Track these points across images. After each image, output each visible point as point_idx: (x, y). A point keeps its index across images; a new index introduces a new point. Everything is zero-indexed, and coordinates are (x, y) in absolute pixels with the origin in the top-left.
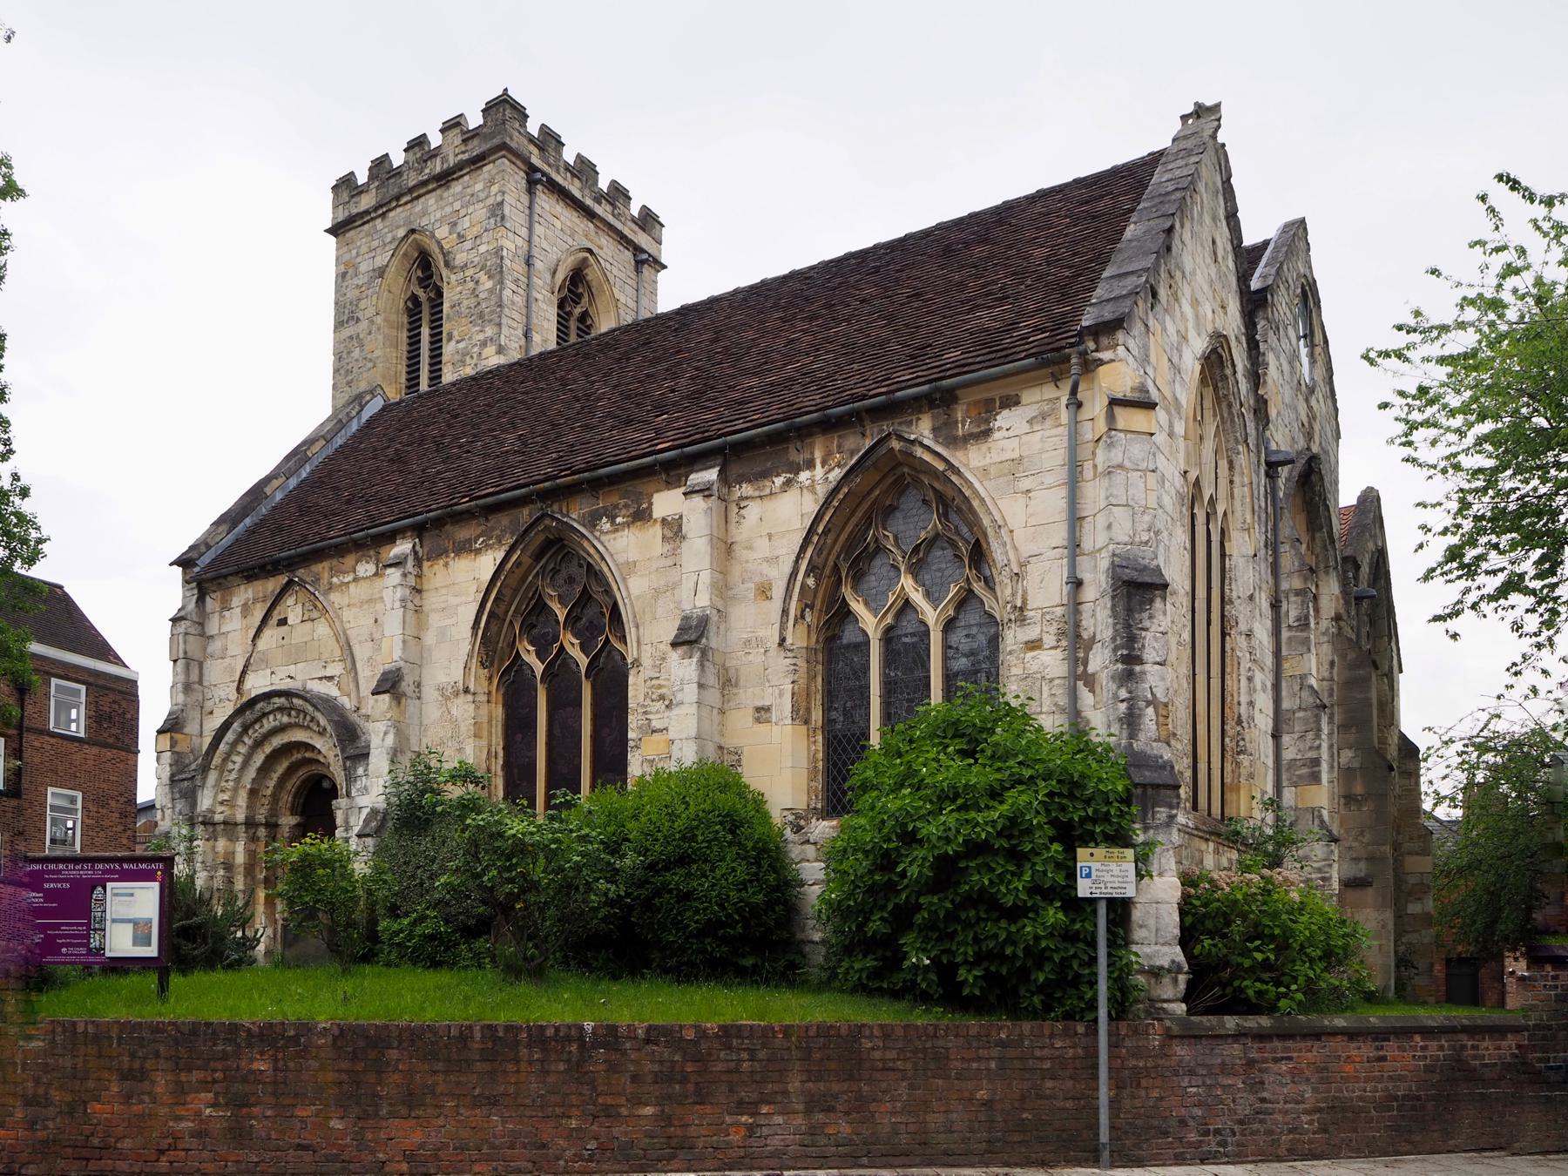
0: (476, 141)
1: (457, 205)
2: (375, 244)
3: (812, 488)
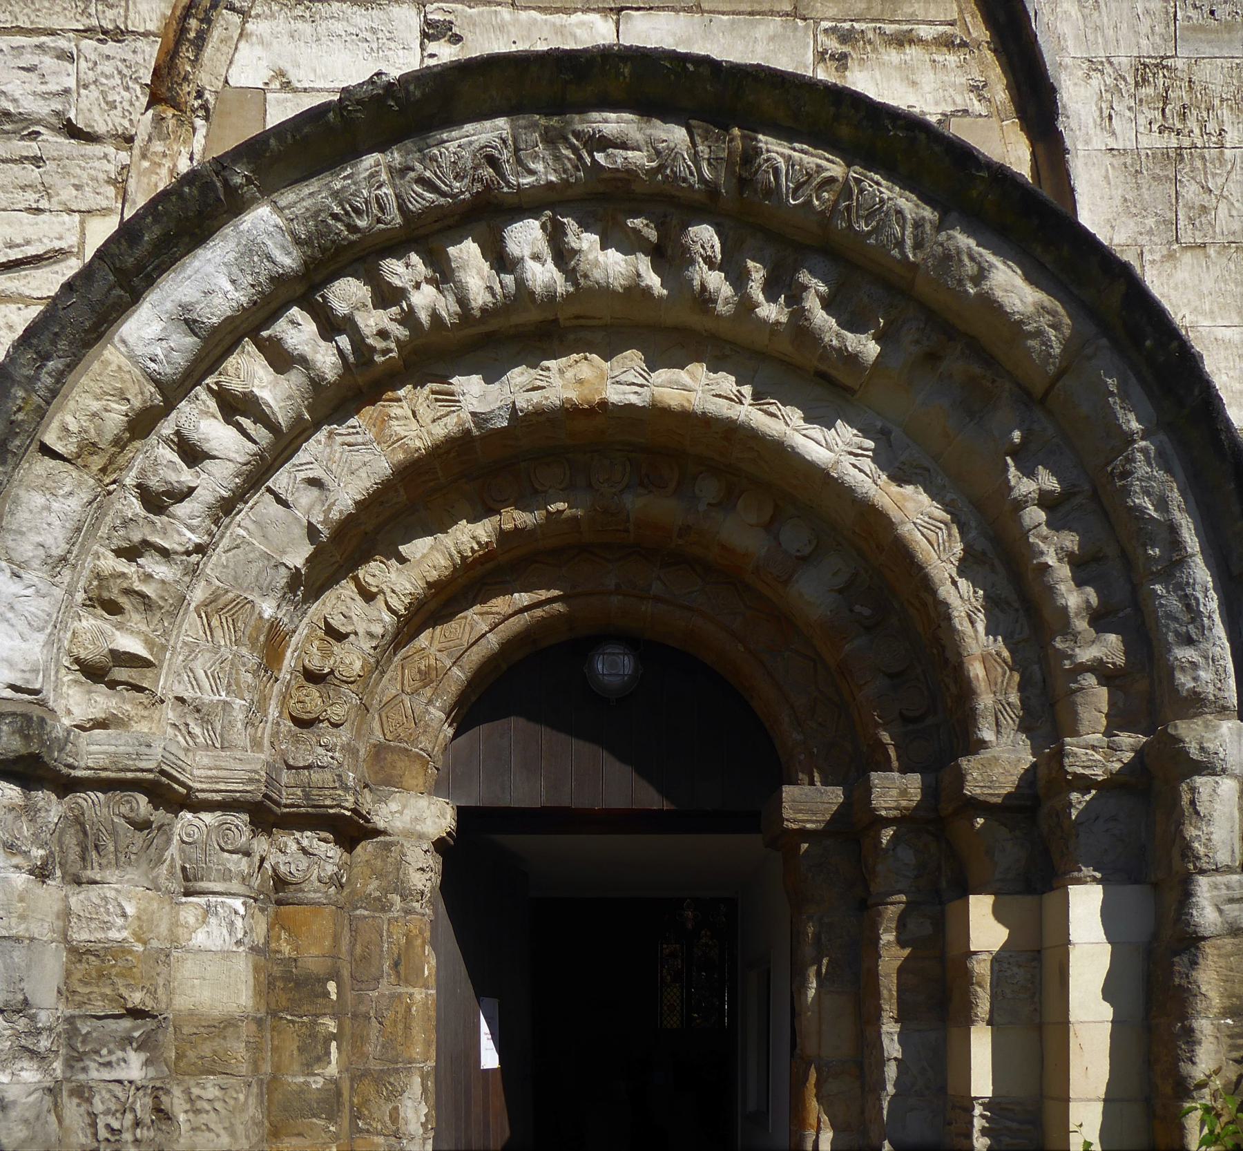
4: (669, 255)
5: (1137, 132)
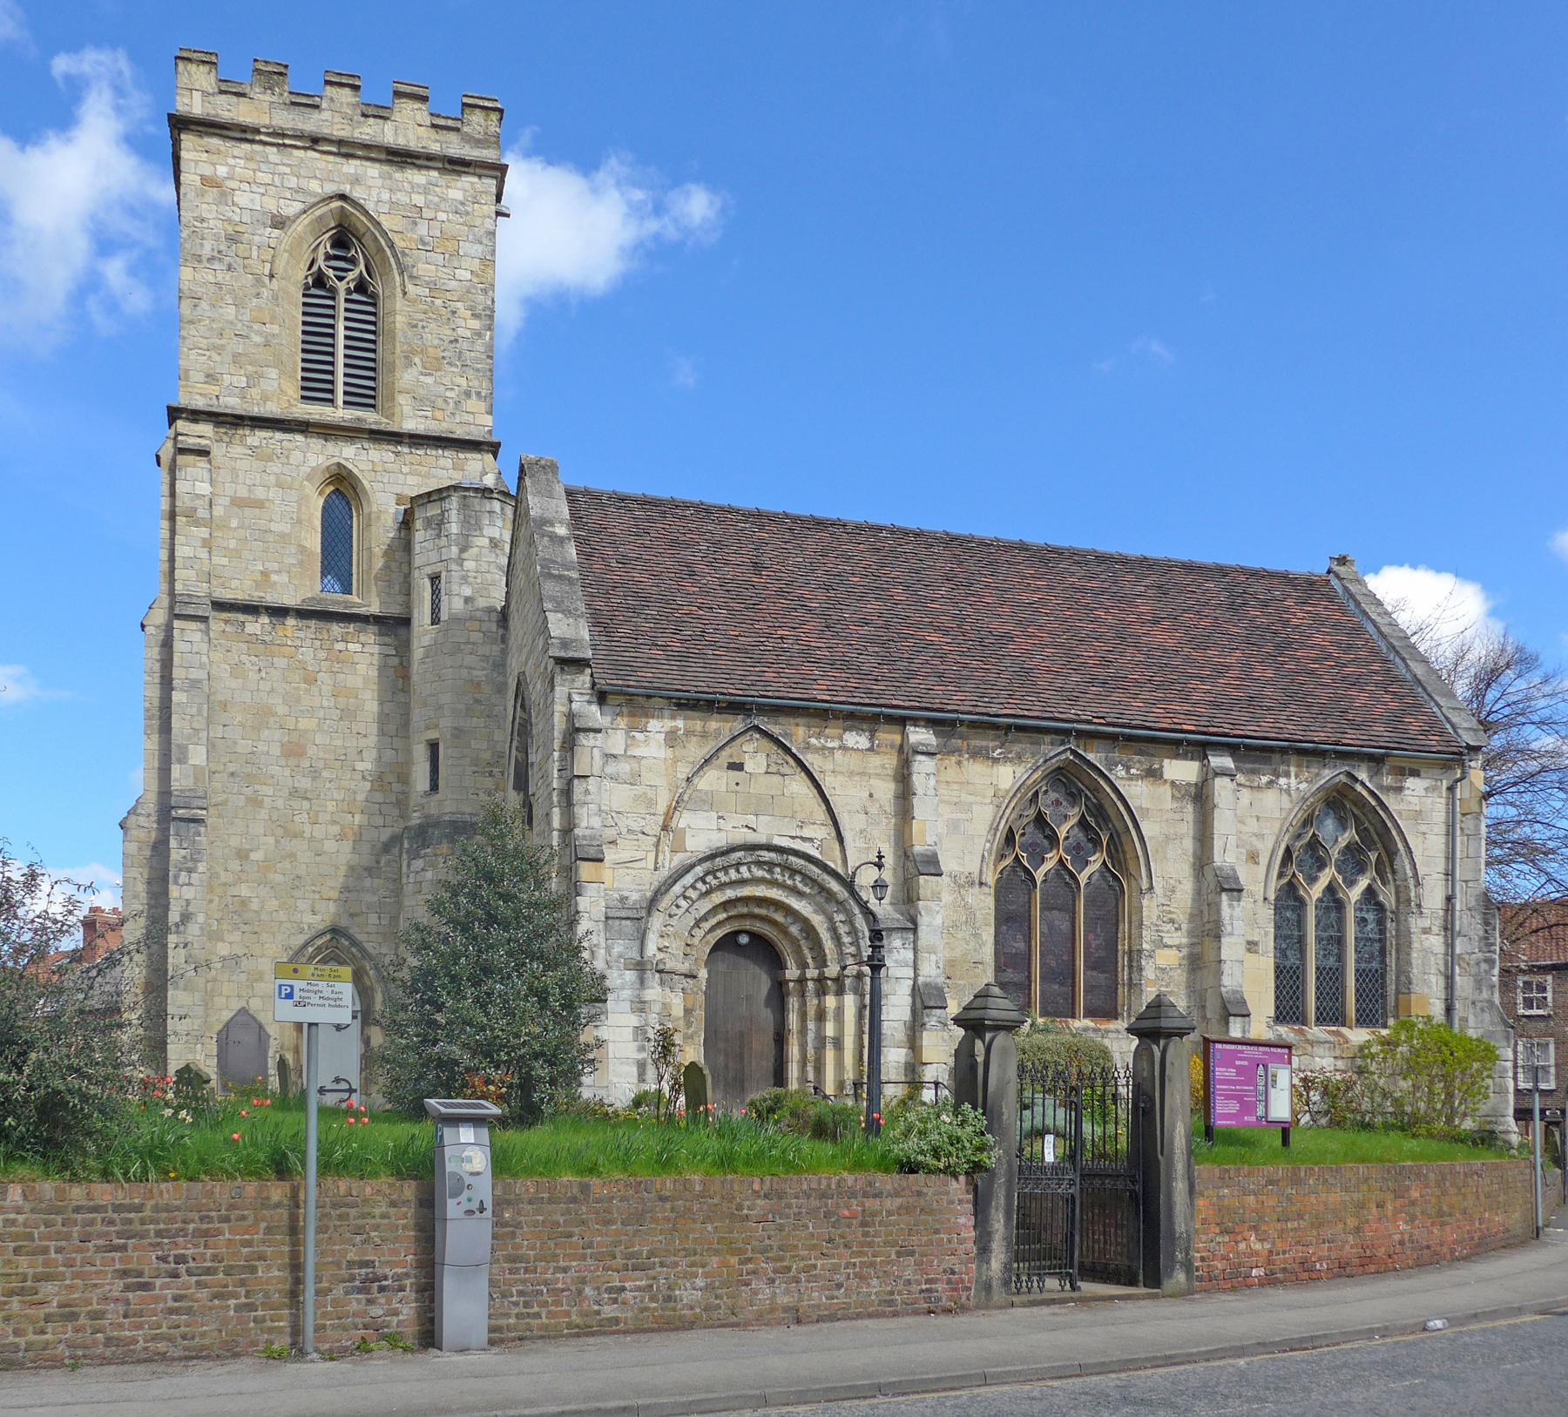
0: (452, 136)
1: (419, 200)
2: (267, 179)
3: (1288, 791)
4: (770, 871)
5: (861, 844)
